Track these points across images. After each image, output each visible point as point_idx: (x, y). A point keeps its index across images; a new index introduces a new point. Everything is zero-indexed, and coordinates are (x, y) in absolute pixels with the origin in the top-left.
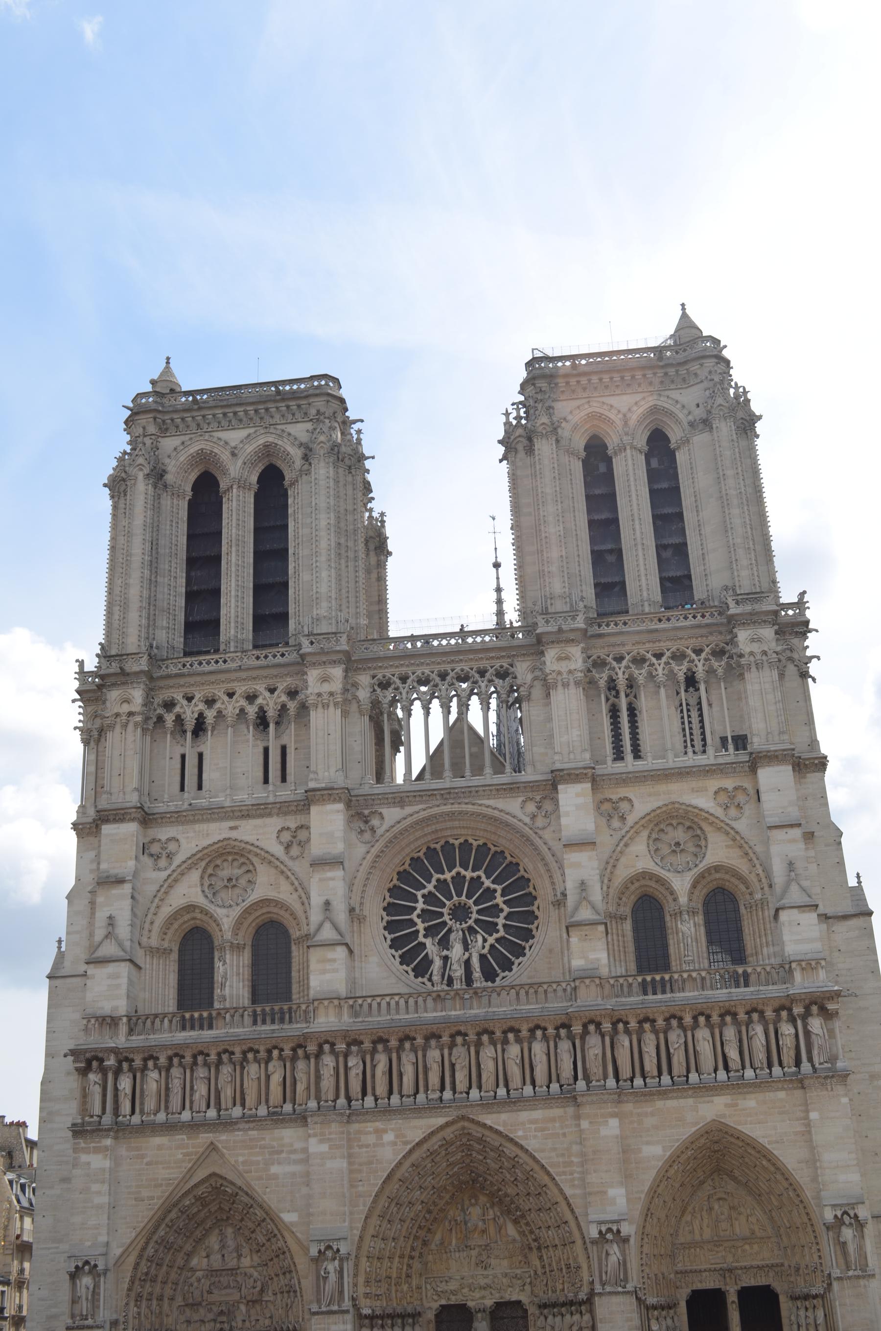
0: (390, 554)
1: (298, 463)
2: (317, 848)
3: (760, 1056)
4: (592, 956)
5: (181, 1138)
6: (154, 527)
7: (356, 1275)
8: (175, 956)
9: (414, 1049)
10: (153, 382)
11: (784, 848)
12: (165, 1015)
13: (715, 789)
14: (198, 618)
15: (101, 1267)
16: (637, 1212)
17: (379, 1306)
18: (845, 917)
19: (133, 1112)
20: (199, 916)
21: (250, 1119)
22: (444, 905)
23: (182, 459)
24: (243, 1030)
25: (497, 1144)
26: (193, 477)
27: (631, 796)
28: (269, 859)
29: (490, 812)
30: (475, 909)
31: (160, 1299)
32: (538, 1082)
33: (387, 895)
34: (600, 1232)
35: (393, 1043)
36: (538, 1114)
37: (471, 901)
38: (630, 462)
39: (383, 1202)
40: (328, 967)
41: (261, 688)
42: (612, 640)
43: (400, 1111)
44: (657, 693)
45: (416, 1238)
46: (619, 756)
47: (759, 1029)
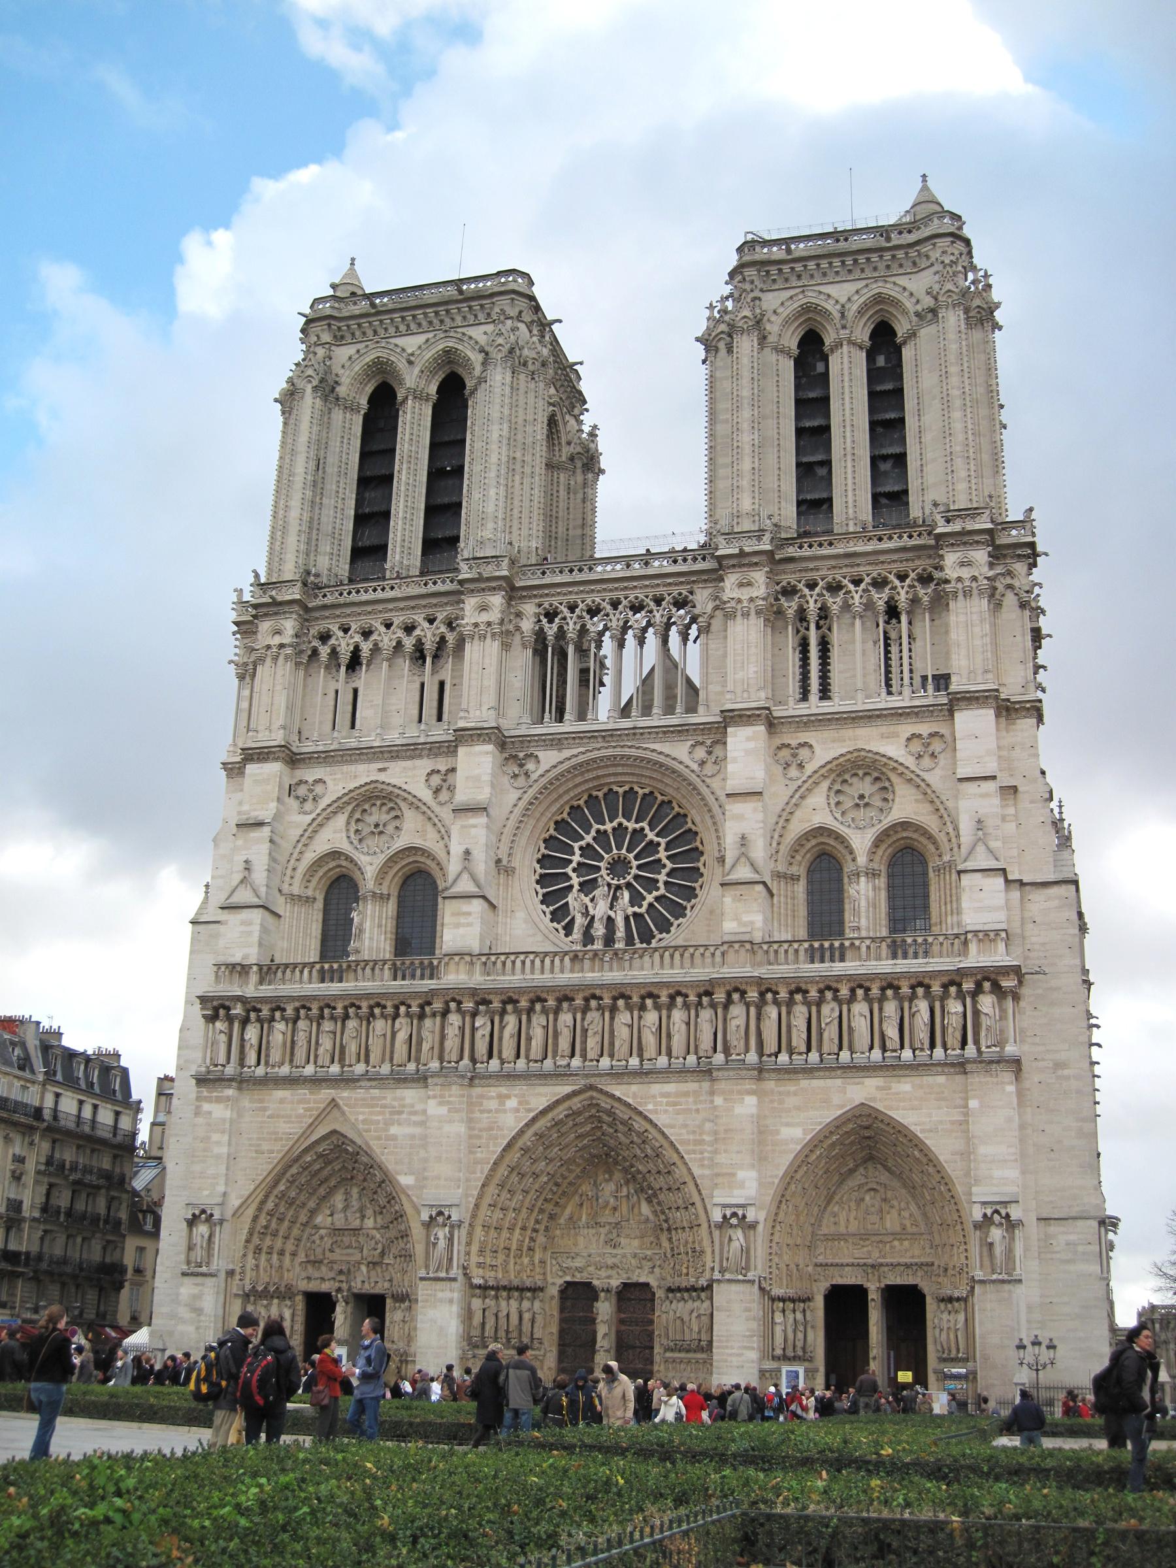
0: (602, 471)
3: (923, 1035)
5: (303, 1092)
6: (320, 445)
7: (469, 1244)
8: (320, 904)
9: (545, 1011)
10: (334, 286)
11: (974, 805)
12: (305, 965)
13: (908, 735)
14: (368, 543)
15: (216, 1216)
16: (769, 1196)
17: (491, 1277)
19: (258, 1064)
20: (344, 863)
24: (383, 983)
25: (626, 1117)
26: (369, 389)
28: (416, 804)
29: (654, 756)
30: (635, 863)
31: (281, 1253)
32: (674, 1054)
33: (543, 846)
34: (724, 1217)
35: (524, 1004)
36: (670, 1088)
37: (631, 856)
38: (846, 360)
39: (503, 1171)
40: (462, 920)
41: (419, 618)
42: (804, 565)
44: (853, 624)
45: (541, 1211)
46: (805, 696)
47: (923, 1006)
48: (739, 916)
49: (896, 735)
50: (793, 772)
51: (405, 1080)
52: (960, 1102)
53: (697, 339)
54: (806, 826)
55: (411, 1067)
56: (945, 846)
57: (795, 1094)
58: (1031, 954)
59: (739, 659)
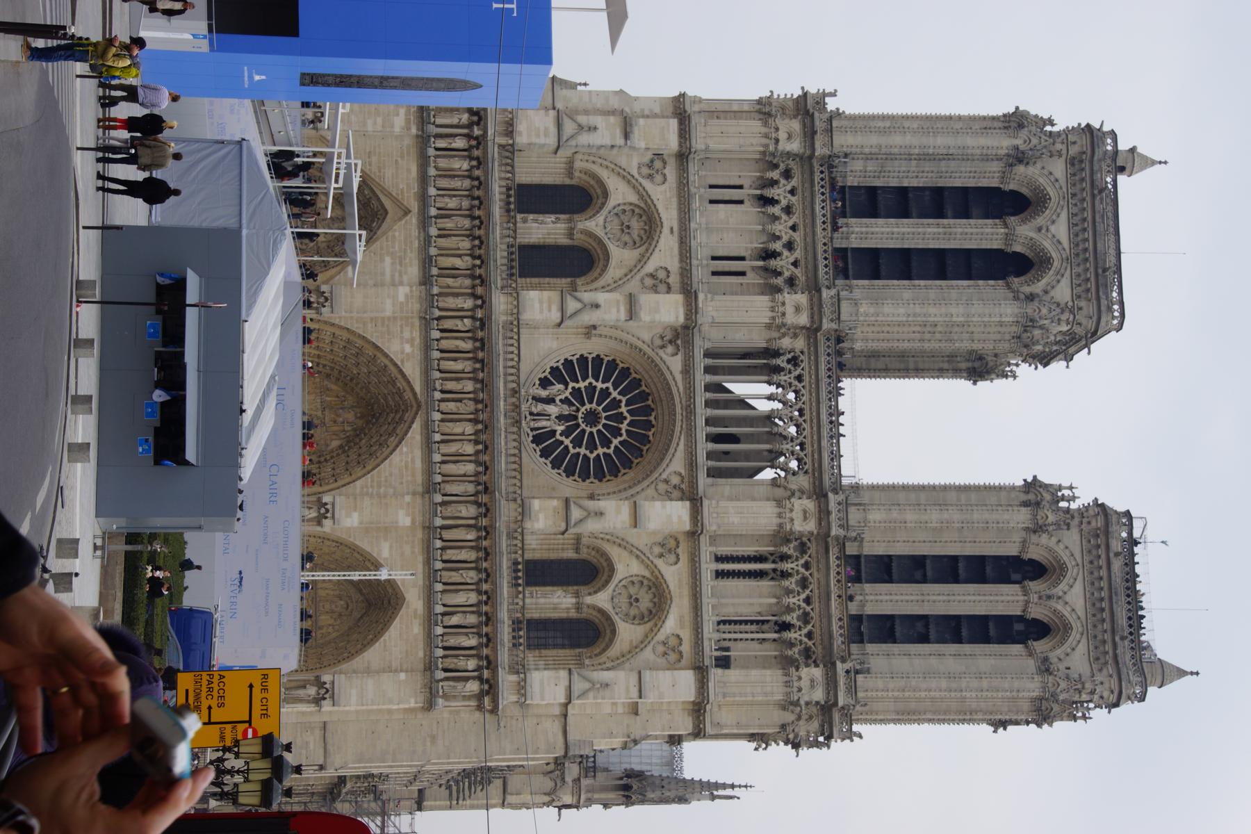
0: (975, 383)
1: (1027, 289)
2: (647, 300)
3: (452, 641)
4: (541, 516)
5: (415, 187)
8: (568, 181)
9: (474, 371)
10: (1133, 150)
11: (621, 682)
13: (682, 636)
18: (565, 732)
19: (437, 149)
21: (427, 241)
22: (599, 404)
23: (1041, 180)
26: (1024, 191)
27: (680, 564)
28: (643, 260)
29: (673, 445)
30: (594, 430)
32: (443, 466)
35: (480, 355)
36: (419, 464)
37: (600, 427)
38: (1009, 598)
39: (359, 342)
40: (545, 305)
41: (798, 254)
42: (823, 561)
43: (427, 359)
45: (332, 369)
46: (719, 559)
47: (473, 642)
48: (546, 512)
49: (682, 627)
50: (657, 550)
51: (424, 267)
52: (405, 667)
53: (1035, 477)
54: (615, 559)
55: (435, 271)
56: (596, 661)
57: (413, 552)
58: (514, 722)
59: (747, 511)
